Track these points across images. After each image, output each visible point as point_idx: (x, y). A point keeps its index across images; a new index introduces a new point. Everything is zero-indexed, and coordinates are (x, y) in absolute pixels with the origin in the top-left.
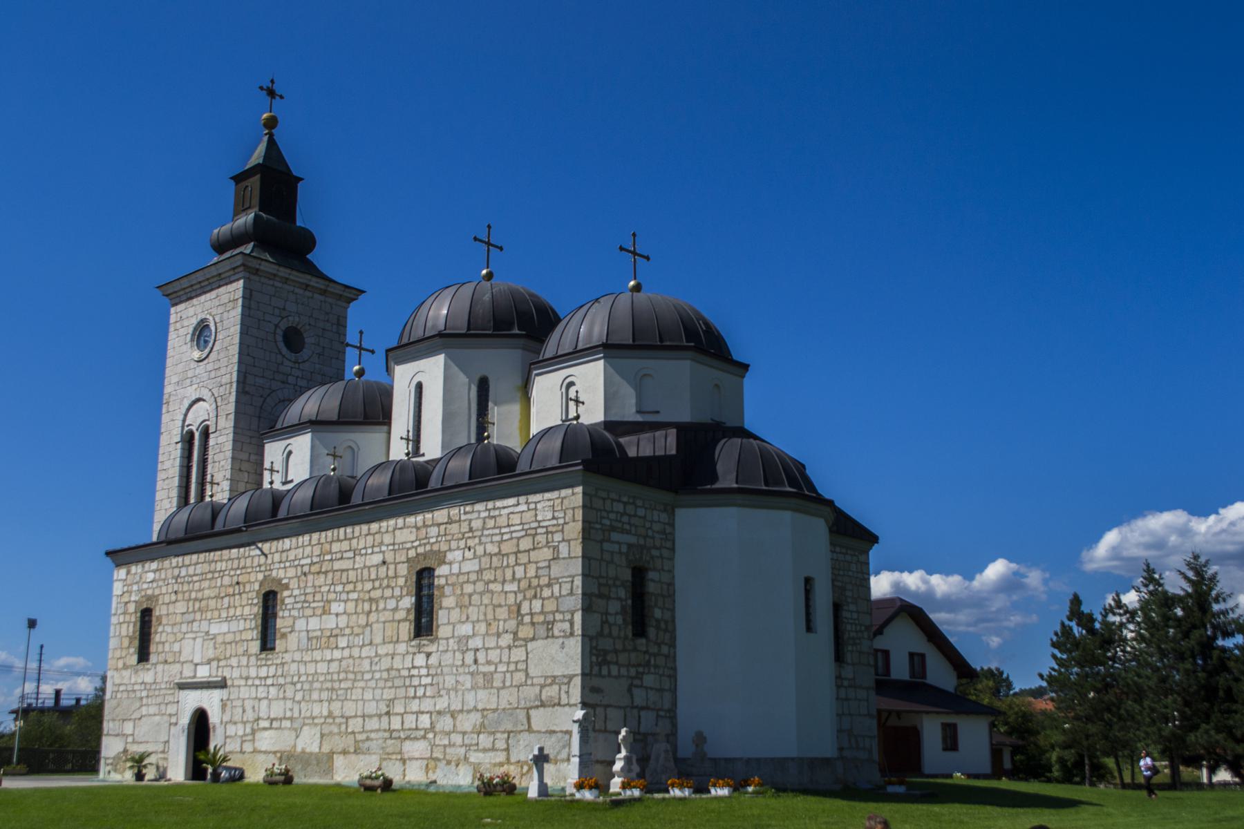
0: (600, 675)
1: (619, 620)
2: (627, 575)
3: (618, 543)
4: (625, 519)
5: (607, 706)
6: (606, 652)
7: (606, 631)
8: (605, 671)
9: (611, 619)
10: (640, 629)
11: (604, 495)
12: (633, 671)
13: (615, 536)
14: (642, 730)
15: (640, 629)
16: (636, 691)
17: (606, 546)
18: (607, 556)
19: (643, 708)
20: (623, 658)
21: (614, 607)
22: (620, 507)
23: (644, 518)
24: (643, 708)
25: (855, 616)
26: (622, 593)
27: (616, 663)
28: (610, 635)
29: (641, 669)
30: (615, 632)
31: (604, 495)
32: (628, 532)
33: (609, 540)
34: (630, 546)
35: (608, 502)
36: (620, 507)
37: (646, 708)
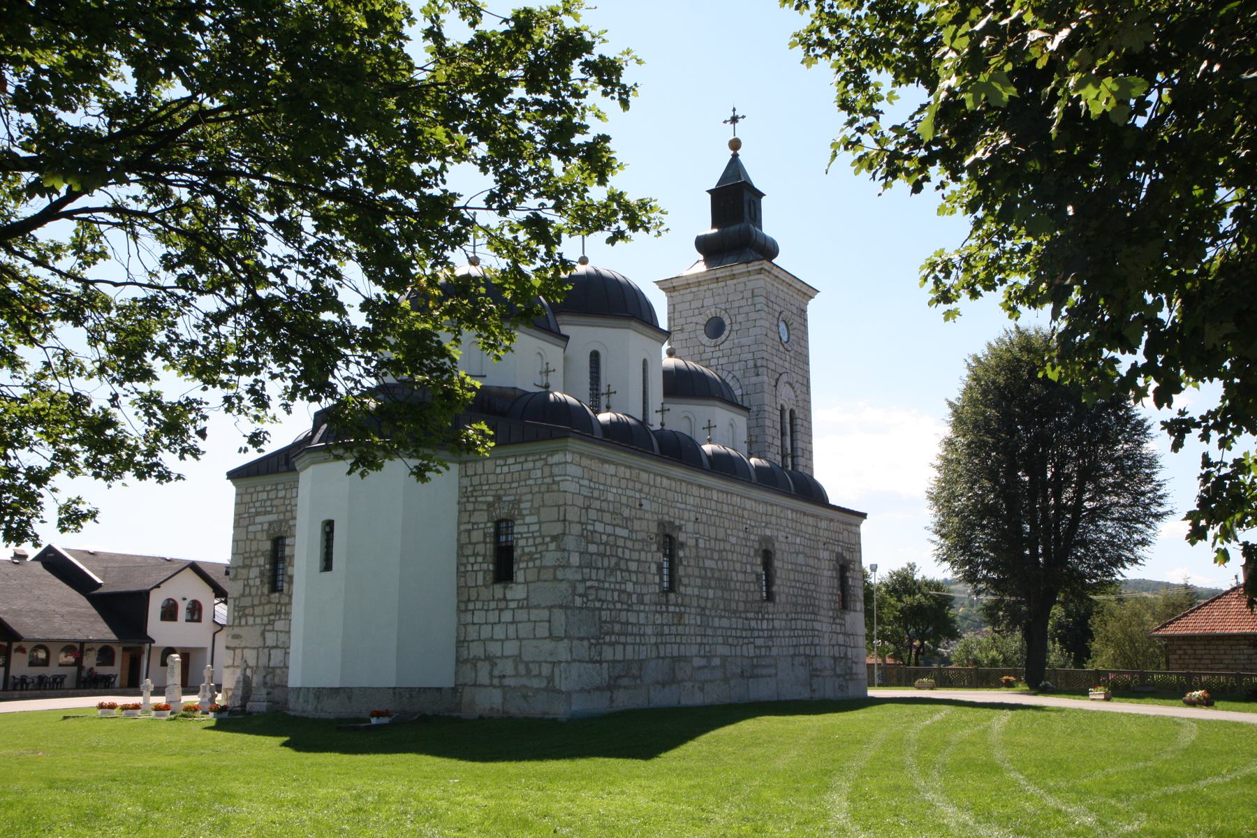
0: (240, 625)
1: (258, 582)
2: (267, 546)
3: (262, 524)
4: (268, 503)
5: (243, 648)
6: (245, 608)
7: (247, 592)
8: (243, 622)
9: (251, 582)
10: (275, 587)
11: (251, 490)
12: (266, 620)
13: (259, 519)
14: (272, 664)
15: (275, 587)
16: (268, 635)
17: (251, 528)
18: (251, 536)
19: (273, 647)
20: (258, 611)
21: (255, 572)
22: (264, 496)
23: (284, 498)
24: (273, 647)
25: (536, 527)
26: (261, 561)
27: (253, 615)
28: (250, 594)
29: (272, 617)
30: (254, 591)
31: (251, 490)
32: (270, 513)
33: (254, 524)
34: (270, 523)
35: (255, 496)
36: (264, 496)
37: (276, 647)
